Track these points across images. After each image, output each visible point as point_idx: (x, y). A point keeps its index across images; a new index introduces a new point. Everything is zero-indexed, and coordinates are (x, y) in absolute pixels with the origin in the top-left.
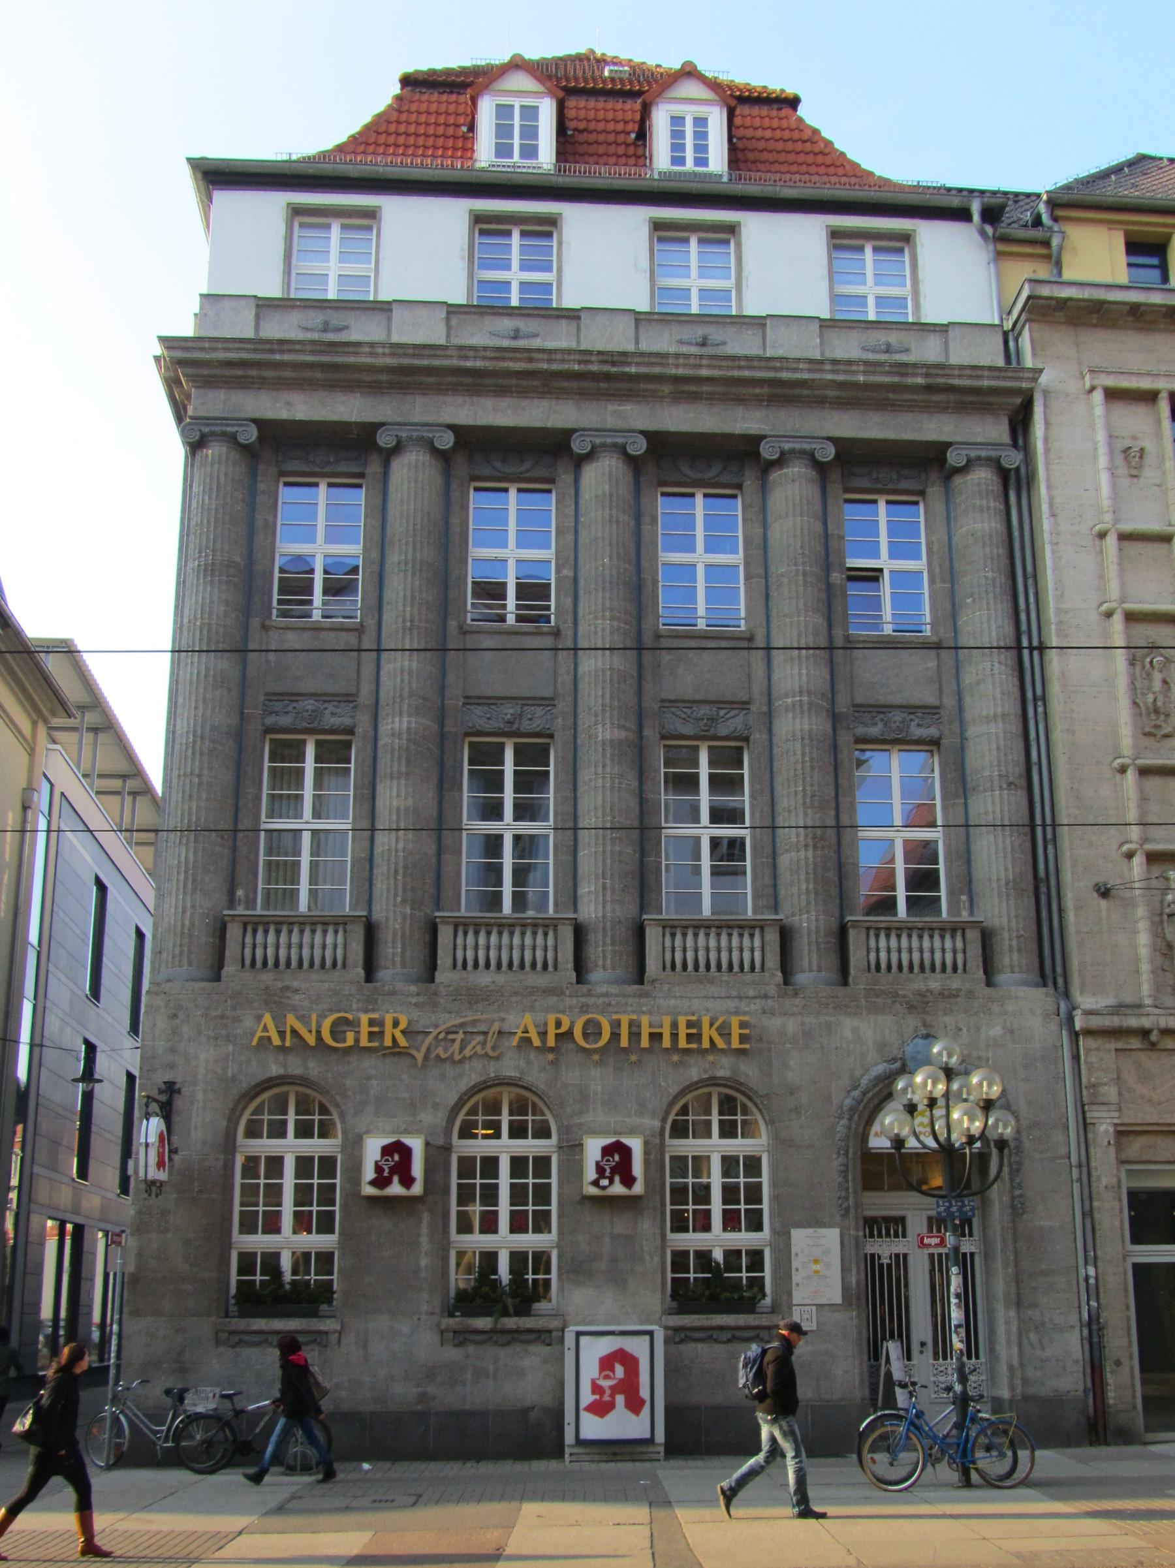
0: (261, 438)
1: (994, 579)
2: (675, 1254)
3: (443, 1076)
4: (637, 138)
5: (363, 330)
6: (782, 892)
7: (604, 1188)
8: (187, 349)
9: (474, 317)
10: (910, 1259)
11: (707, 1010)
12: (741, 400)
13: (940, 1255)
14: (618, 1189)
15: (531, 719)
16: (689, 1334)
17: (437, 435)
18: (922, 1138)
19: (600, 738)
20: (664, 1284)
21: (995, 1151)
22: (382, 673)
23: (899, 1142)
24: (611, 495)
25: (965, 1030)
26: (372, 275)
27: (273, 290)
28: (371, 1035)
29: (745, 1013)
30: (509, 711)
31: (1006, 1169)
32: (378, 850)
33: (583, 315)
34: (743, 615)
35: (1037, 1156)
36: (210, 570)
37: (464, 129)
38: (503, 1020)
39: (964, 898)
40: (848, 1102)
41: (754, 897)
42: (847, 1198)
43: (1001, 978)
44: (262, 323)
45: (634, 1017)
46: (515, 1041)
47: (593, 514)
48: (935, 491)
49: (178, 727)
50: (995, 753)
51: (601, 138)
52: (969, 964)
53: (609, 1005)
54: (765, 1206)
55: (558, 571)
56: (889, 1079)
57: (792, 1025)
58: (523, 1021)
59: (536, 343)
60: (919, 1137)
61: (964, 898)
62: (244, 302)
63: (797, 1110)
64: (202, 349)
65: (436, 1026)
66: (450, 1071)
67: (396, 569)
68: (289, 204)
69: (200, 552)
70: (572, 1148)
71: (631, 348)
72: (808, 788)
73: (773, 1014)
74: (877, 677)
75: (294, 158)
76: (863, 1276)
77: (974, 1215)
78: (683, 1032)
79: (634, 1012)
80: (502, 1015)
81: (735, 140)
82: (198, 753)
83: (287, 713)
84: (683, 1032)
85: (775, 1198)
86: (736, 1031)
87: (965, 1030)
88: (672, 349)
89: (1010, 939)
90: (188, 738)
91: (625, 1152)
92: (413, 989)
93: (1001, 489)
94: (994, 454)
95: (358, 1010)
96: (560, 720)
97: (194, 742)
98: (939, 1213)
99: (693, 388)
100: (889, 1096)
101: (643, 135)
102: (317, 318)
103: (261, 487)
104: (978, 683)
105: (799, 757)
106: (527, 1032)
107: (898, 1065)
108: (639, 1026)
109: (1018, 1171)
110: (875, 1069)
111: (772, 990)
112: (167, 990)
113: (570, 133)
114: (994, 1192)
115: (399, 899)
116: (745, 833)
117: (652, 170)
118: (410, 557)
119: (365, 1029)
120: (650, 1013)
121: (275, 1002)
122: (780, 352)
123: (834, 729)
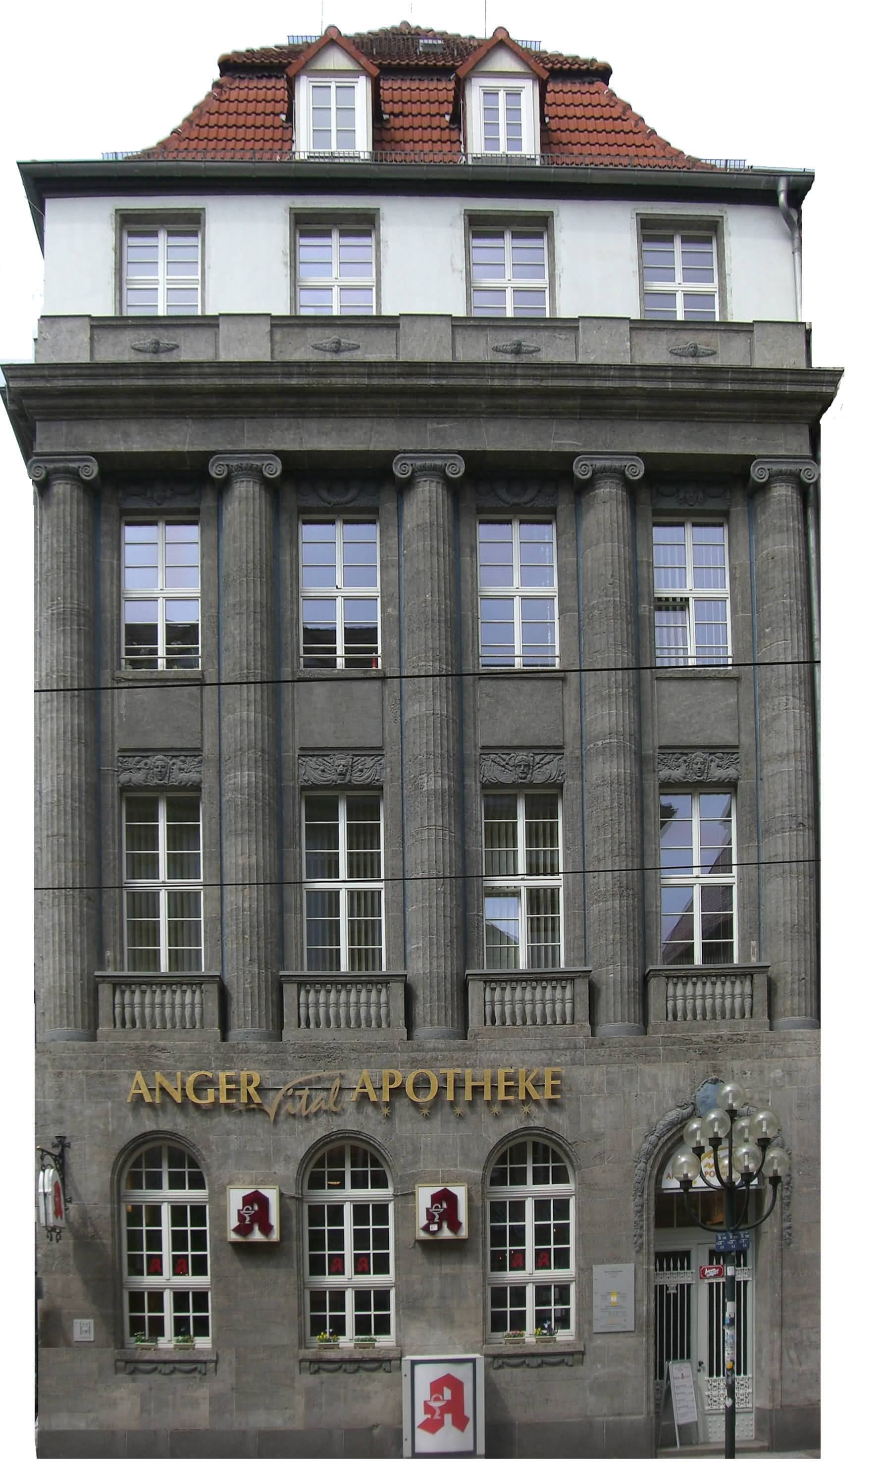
0: (101, 473)
1: (791, 605)
2: (494, 1291)
3: (292, 1131)
4: (451, 121)
5: (192, 349)
6: (591, 943)
7: (434, 1233)
8: (29, 378)
9: (297, 330)
10: (693, 1288)
11: (524, 1062)
12: (553, 414)
13: (718, 1284)
14: (446, 1233)
15: (361, 771)
16: (505, 1360)
17: (266, 463)
18: (708, 1177)
19: (425, 788)
20: (484, 1318)
21: (770, 1187)
22: (223, 725)
23: (686, 1183)
24: (431, 524)
25: (749, 1073)
26: (199, 287)
27: (105, 308)
28: (229, 1092)
29: (556, 1065)
30: (341, 761)
31: (778, 1203)
32: (227, 909)
33: (401, 322)
34: (557, 653)
35: (805, 1190)
36: (61, 618)
37: (283, 117)
38: (342, 1077)
39: (753, 943)
40: (646, 1146)
41: (566, 949)
42: (641, 1236)
43: (780, 1021)
44: (96, 344)
45: (459, 1071)
46: (353, 1096)
47: (415, 546)
48: (738, 511)
49: (44, 786)
50: (786, 792)
51: (417, 122)
52: (755, 1009)
53: (437, 1059)
54: (572, 1245)
55: (383, 612)
56: (683, 1122)
57: (598, 1074)
58: (360, 1077)
59: (357, 356)
60: (706, 1180)
61: (753, 943)
62: (78, 322)
63: (601, 1156)
64: (43, 377)
65: (285, 1084)
66: (299, 1126)
67: (232, 612)
68: (117, 210)
69: (52, 601)
70: (407, 1196)
71: (447, 358)
72: (616, 835)
73: (582, 1064)
74: (682, 716)
75: (120, 158)
76: (652, 1305)
77: (748, 1247)
78: (502, 1085)
79: (458, 1066)
80: (343, 1072)
81: (547, 120)
82: (62, 813)
83: (139, 769)
84: (502, 1085)
85: (579, 1238)
86: (548, 1083)
87: (749, 1073)
88: (488, 359)
89: (793, 983)
90: (53, 797)
91: (451, 1199)
92: (264, 1047)
93: (801, 506)
94: (793, 468)
95: (217, 1068)
96: (388, 770)
97: (58, 800)
98: (718, 1247)
99: (508, 402)
100: (681, 1140)
101: (458, 118)
102: (146, 338)
103: (105, 527)
104: (775, 718)
105: (608, 803)
106: (365, 1087)
107: (689, 1109)
108: (463, 1080)
109: (788, 1204)
110: (670, 1114)
111: (581, 1040)
112: (52, 1049)
113: (385, 117)
114: (766, 1226)
115: (248, 959)
116: (556, 881)
117: (466, 155)
118: (244, 598)
119: (223, 1087)
120: (473, 1066)
121: (145, 1062)
122: (592, 359)
123: (641, 772)
